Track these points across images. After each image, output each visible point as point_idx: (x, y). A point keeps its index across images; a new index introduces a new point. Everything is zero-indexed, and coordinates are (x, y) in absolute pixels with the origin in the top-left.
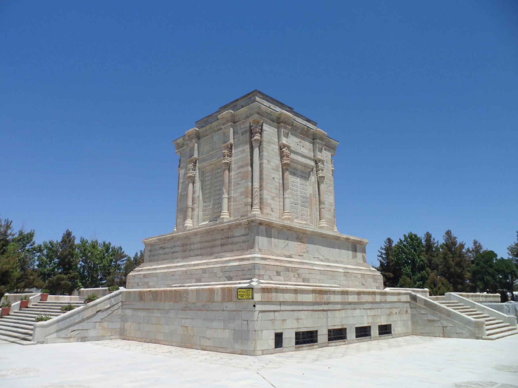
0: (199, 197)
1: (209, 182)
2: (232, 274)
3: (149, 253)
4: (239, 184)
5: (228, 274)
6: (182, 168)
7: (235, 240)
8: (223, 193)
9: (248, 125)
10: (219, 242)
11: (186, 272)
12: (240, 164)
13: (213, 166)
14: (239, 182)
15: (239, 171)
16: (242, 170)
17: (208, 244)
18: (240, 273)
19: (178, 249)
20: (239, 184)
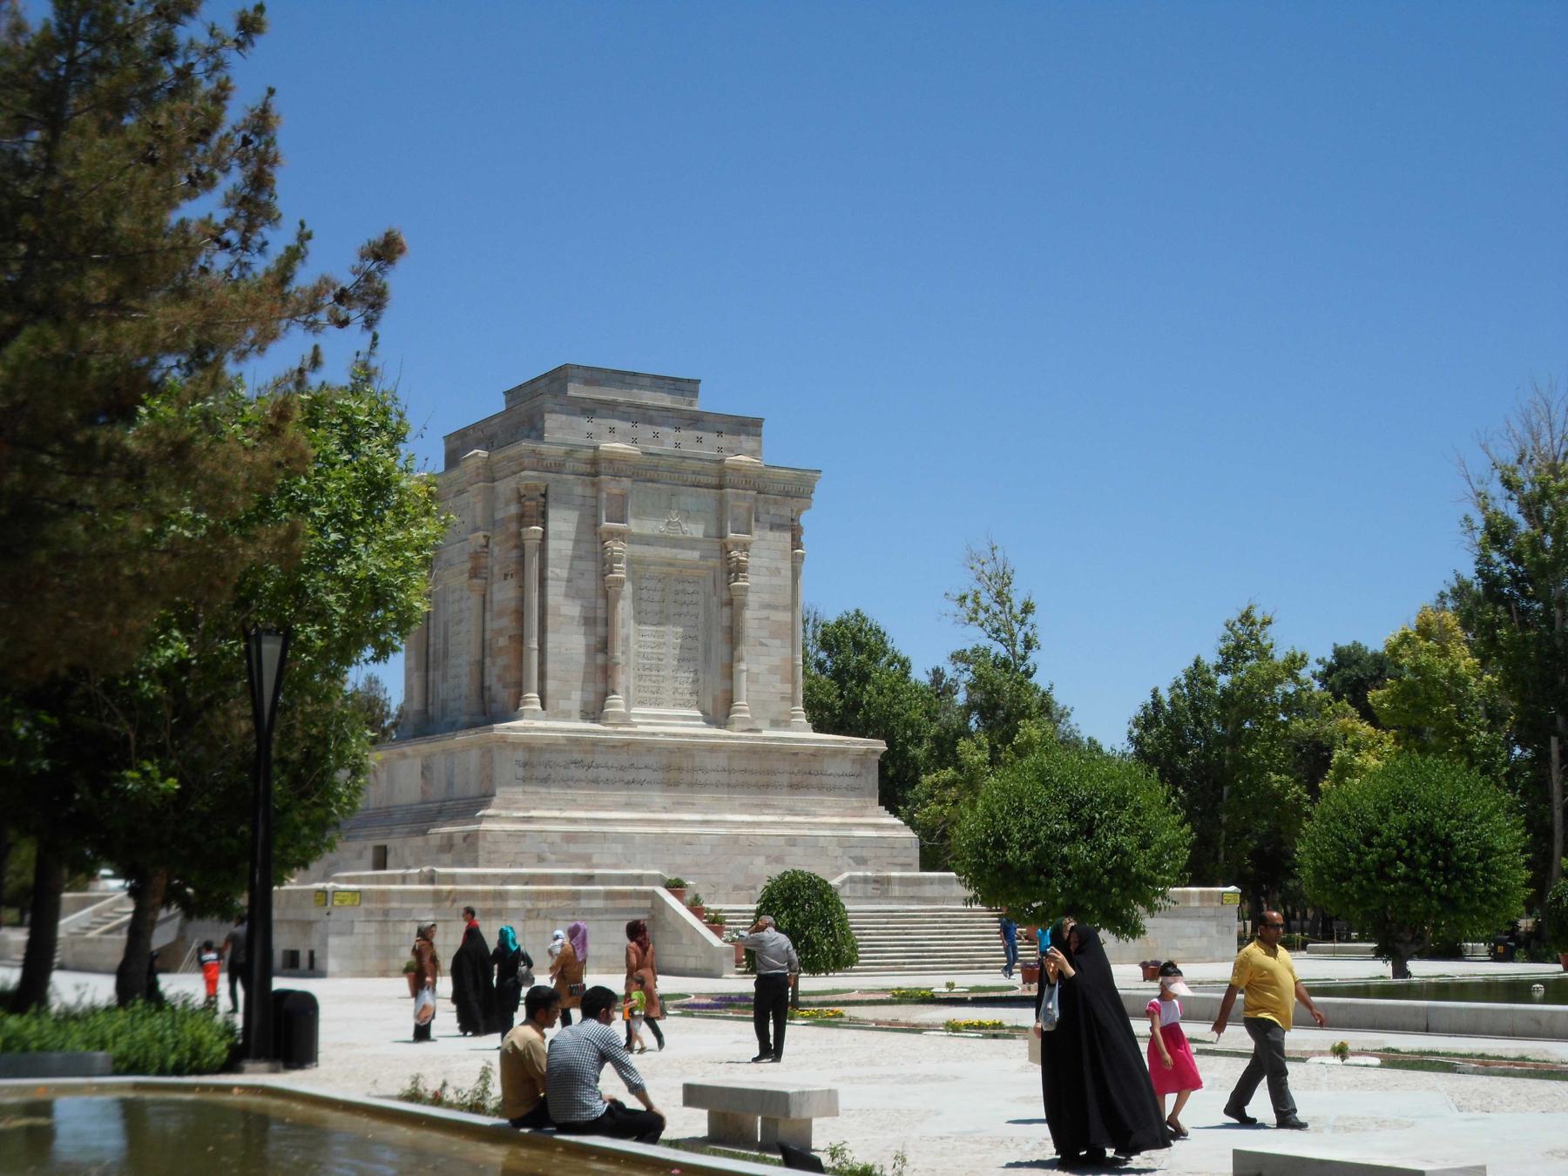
1: (656, 607)
2: (865, 853)
3: (520, 772)
4: (762, 644)
5: (856, 852)
6: (559, 537)
7: (826, 780)
8: (740, 660)
10: (784, 779)
11: (735, 839)
12: (767, 598)
13: (671, 569)
15: (765, 613)
17: (753, 779)
18: (887, 852)
19: (643, 775)
20: (762, 644)
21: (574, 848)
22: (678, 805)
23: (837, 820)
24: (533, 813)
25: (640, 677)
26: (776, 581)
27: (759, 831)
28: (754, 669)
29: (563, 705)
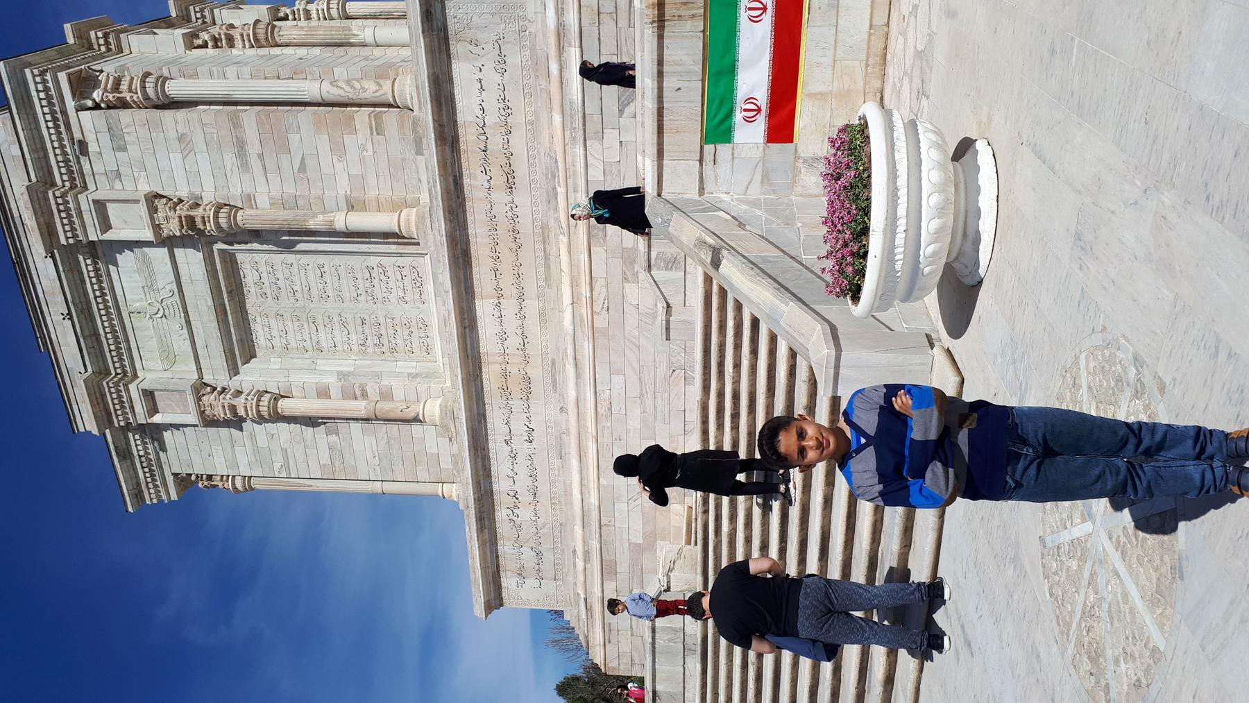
0: (342, 375)
3: (531, 582)
4: (303, 167)
7: (492, 119)
9: (85, 116)
10: (500, 197)
12: (230, 159)
14: (296, 167)
16: (253, 149)
19: (518, 427)
20: (303, 167)
21: (623, 567)
22: (555, 383)
23: (557, 118)
24: (582, 596)
25: (393, 351)
26: (199, 139)
27: (584, 290)
28: (343, 187)
29: (446, 463)
